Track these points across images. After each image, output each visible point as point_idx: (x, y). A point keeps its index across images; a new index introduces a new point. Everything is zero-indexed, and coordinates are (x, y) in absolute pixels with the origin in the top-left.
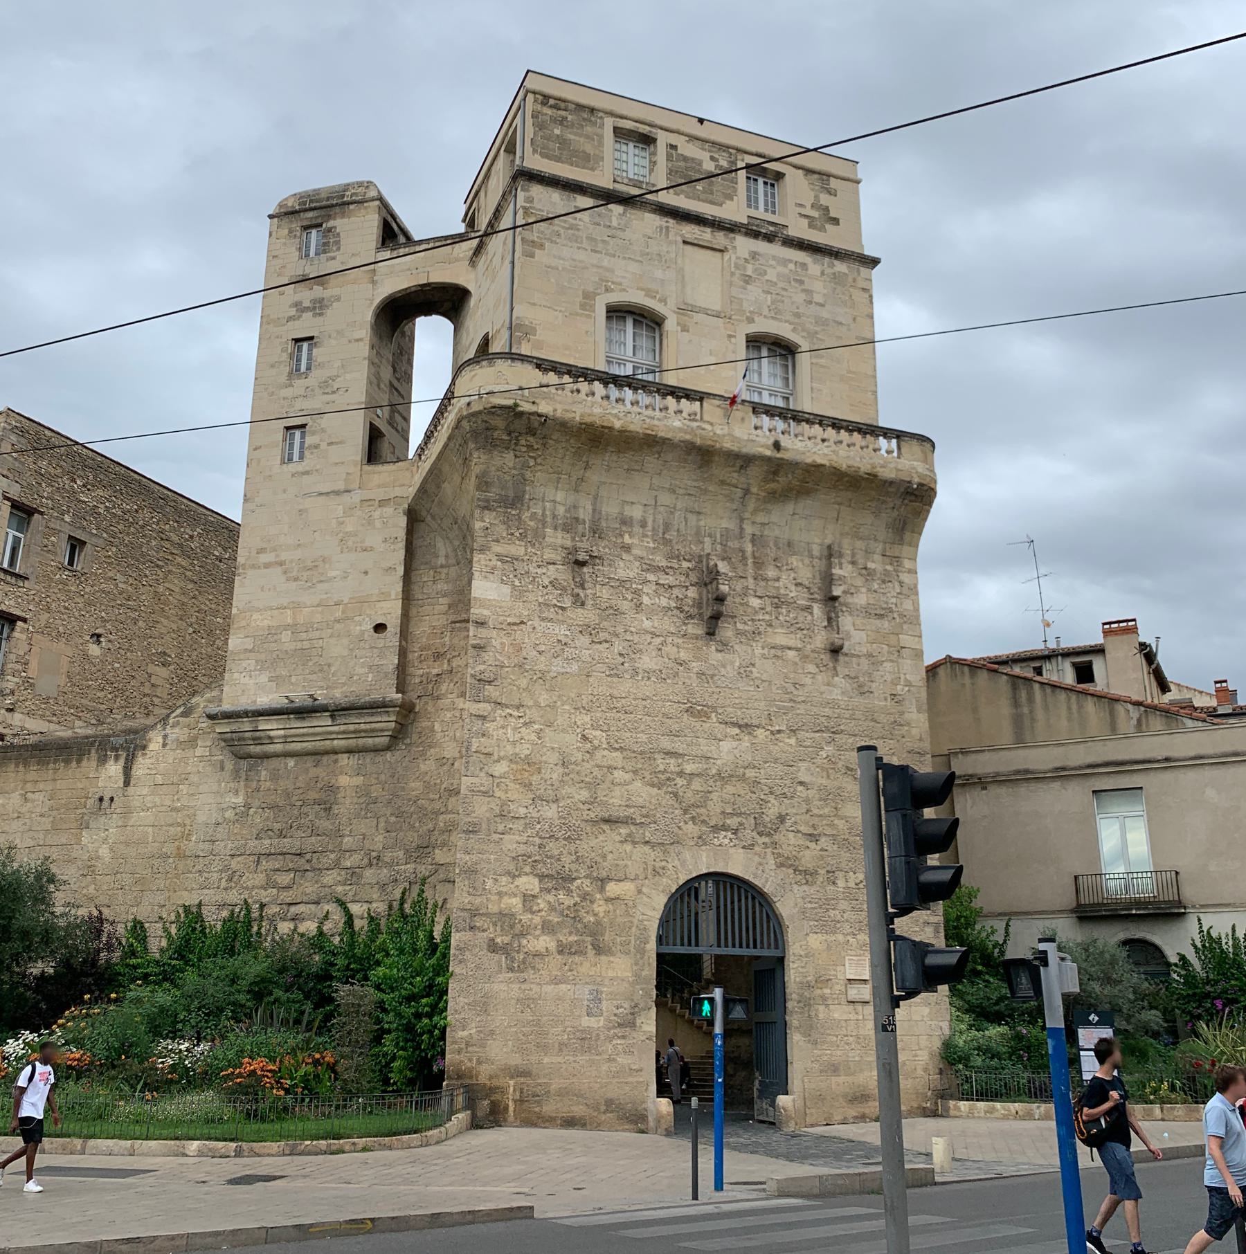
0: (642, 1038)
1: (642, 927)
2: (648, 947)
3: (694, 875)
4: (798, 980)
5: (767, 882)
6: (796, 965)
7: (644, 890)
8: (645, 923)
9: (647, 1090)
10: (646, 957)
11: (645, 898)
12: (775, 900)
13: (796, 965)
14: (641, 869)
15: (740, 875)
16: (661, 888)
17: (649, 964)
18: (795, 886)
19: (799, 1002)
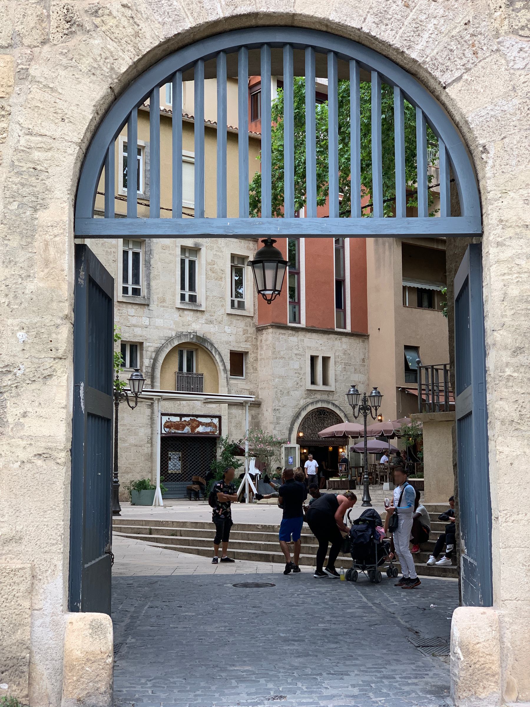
0: (23, 455)
1: (26, 166)
2: (43, 216)
3: (188, 24)
4: (514, 291)
5: (418, 30)
6: (508, 253)
7: (35, 70)
8: (36, 155)
9: (31, 591)
10: (38, 244)
11: (36, 93)
12: (444, 79)
13: (508, 253)
14: (32, 21)
15: (334, 17)
16: (85, 64)
17: (47, 263)
18: (510, 40)
19: (518, 351)
